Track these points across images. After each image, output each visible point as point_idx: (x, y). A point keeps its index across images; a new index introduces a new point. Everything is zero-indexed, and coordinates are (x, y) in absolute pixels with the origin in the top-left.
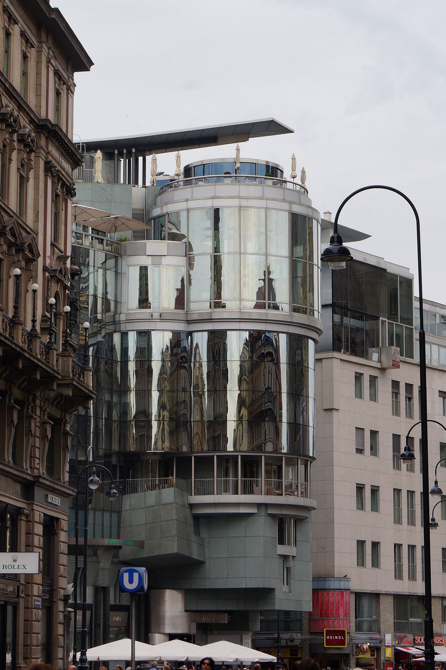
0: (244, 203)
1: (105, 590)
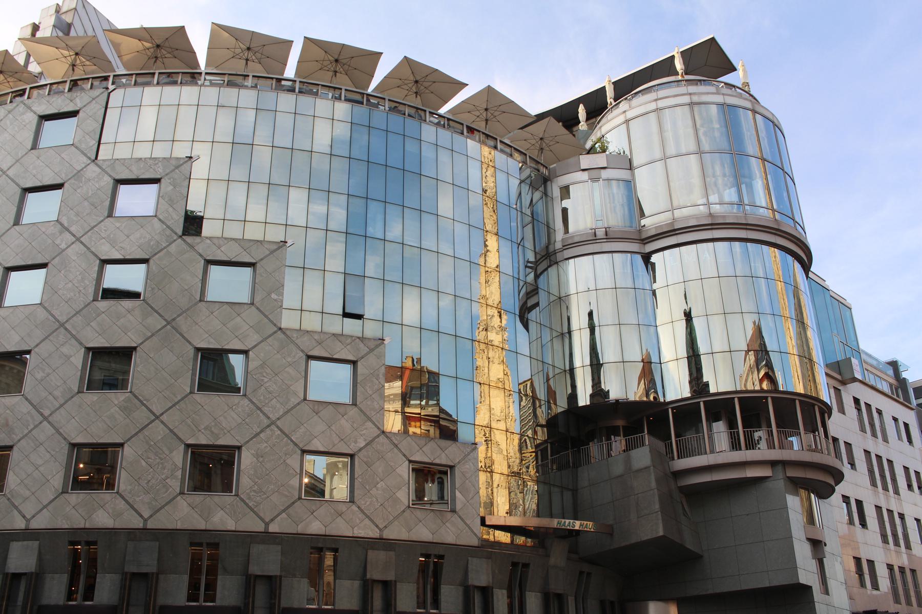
0: (695, 99)
1: (560, 597)
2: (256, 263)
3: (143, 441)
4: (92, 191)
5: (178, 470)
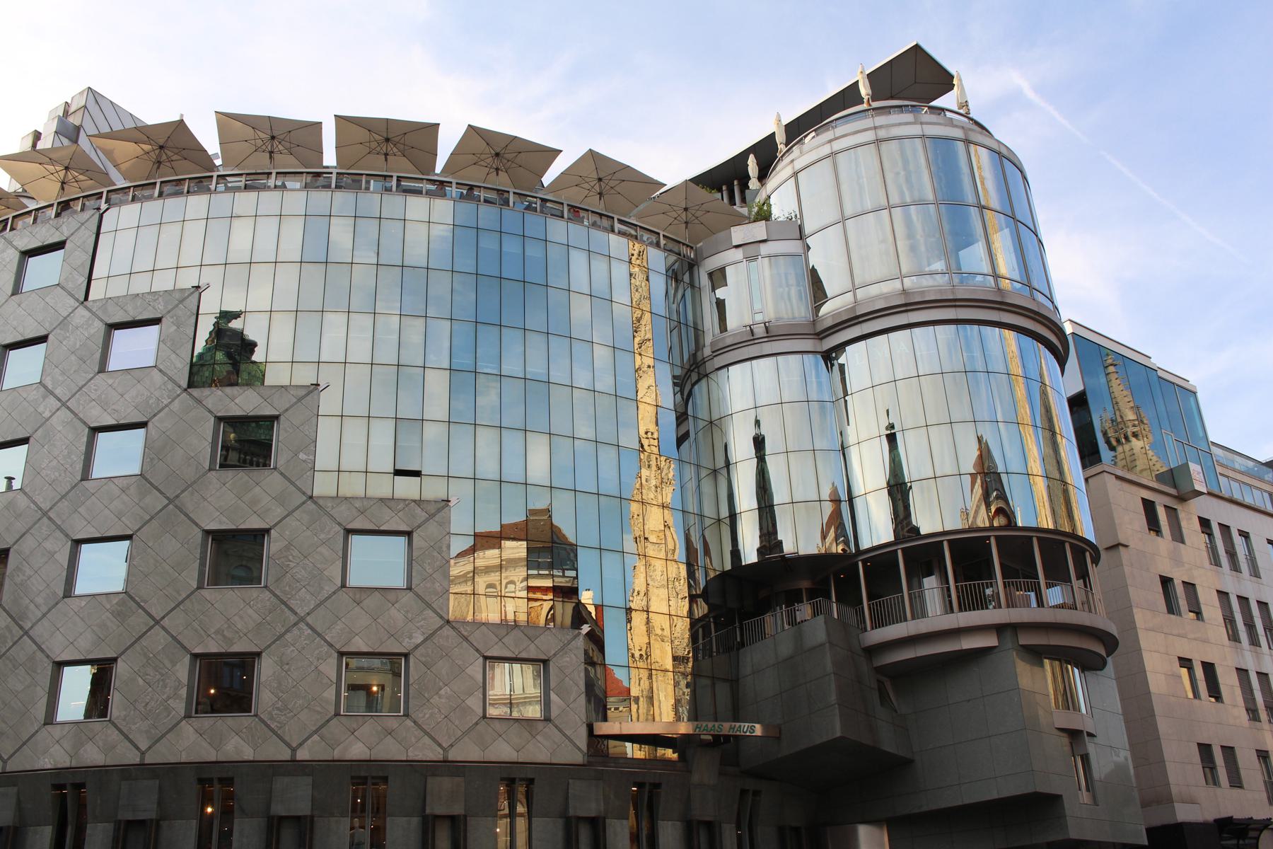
0: (882, 134)
1: (709, 825)
2: (280, 415)
3: (139, 653)
4: (80, 341)
5: (182, 688)
